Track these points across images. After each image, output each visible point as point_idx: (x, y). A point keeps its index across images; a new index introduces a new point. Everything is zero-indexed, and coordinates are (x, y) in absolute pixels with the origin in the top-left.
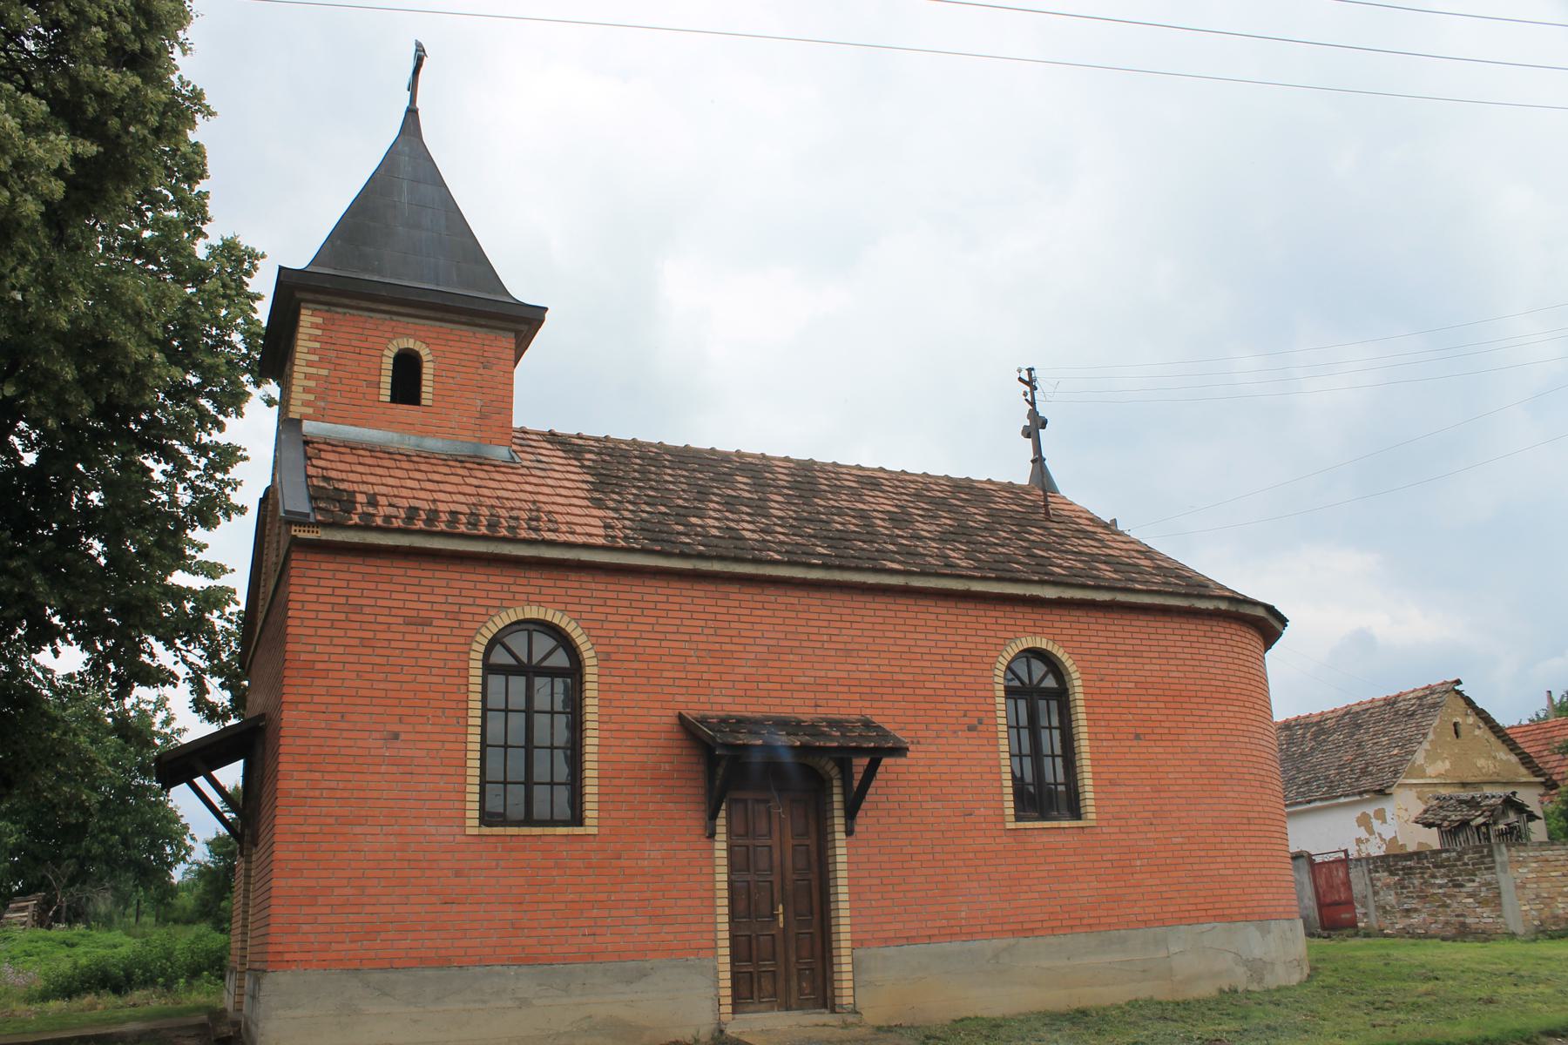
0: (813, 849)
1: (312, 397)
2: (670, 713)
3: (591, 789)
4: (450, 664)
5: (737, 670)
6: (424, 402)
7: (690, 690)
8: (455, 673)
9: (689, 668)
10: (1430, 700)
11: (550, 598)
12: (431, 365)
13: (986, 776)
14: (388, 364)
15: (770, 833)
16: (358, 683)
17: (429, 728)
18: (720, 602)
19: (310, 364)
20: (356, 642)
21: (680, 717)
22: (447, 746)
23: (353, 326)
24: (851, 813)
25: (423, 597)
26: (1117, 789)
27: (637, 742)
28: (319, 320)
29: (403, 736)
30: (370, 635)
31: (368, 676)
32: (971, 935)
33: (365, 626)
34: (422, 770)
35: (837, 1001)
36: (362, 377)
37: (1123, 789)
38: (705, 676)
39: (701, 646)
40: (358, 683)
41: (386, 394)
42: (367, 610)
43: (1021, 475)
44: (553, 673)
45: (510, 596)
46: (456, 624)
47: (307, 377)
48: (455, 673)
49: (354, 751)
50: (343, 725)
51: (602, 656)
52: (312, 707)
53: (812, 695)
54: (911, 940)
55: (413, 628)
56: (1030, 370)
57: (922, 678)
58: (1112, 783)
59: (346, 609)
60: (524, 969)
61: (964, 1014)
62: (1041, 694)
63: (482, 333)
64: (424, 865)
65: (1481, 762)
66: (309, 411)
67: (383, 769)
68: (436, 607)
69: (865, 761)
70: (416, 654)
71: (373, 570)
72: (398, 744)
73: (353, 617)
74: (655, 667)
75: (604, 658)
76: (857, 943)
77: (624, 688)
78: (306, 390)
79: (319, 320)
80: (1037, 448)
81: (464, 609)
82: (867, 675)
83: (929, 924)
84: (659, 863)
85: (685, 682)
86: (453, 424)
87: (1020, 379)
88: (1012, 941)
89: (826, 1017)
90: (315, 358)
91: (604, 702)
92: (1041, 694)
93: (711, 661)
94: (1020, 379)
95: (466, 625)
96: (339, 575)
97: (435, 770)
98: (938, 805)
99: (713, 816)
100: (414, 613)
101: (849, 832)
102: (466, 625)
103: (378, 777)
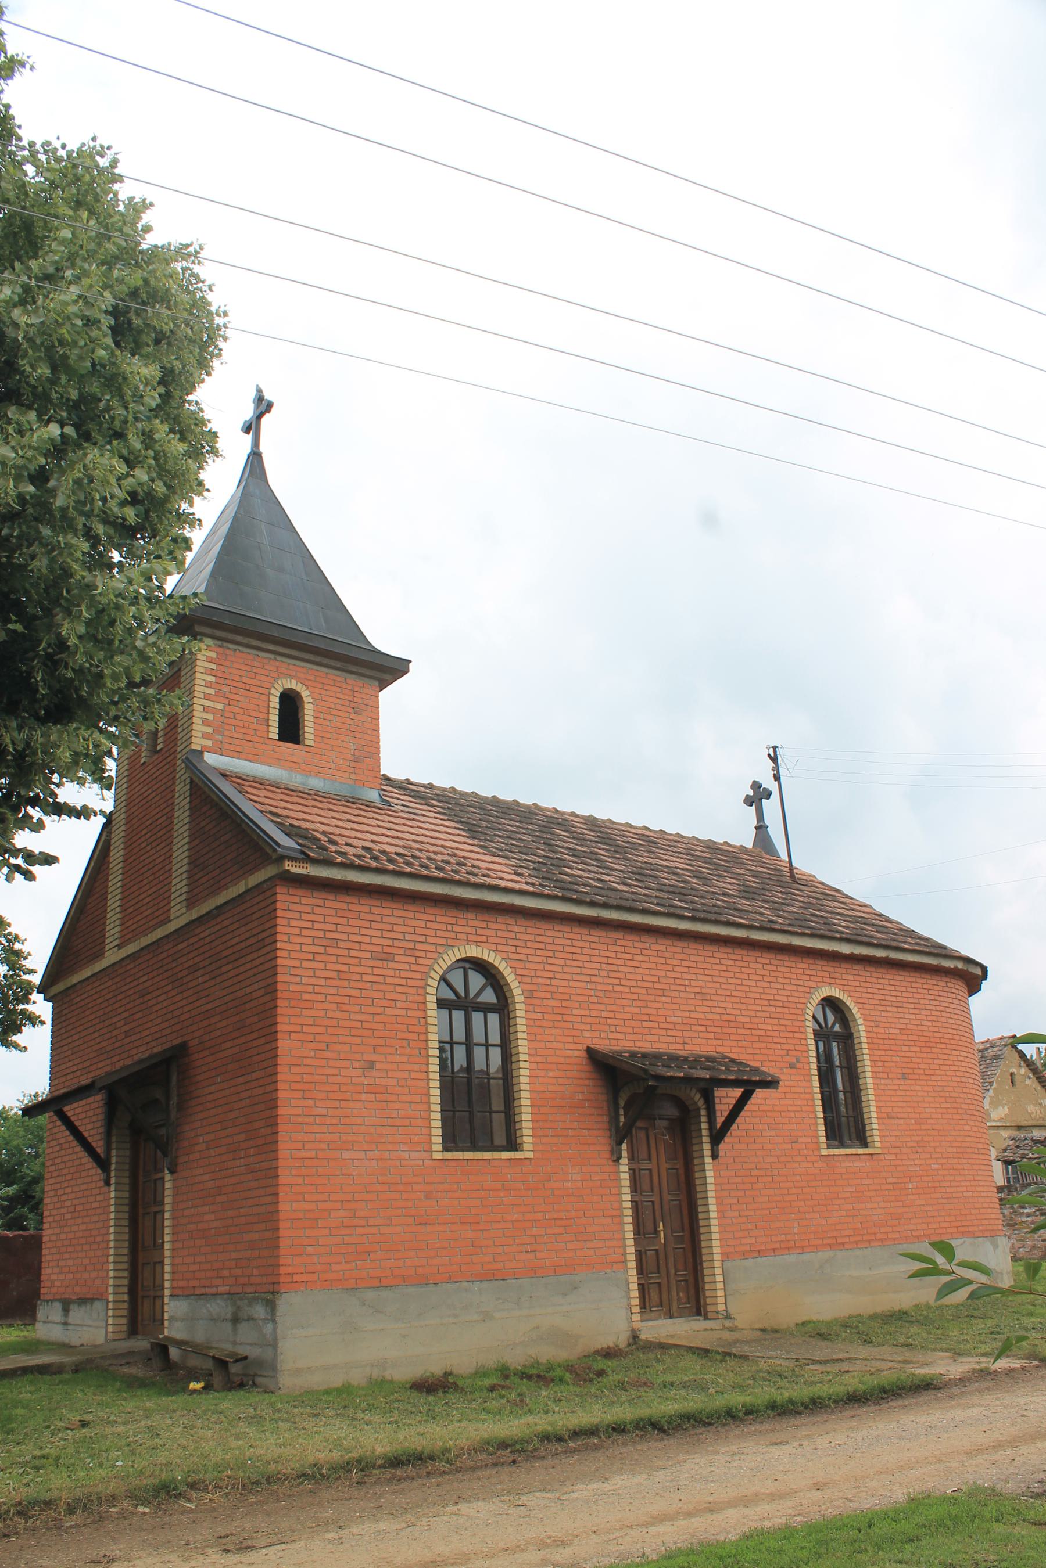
0: (681, 1172)
1: (210, 730)
2: (580, 1047)
3: (526, 1116)
4: (411, 998)
5: (627, 1009)
6: (307, 742)
7: (594, 1027)
8: (415, 1006)
9: (591, 1006)
10: (991, 1052)
11: (484, 939)
12: (311, 706)
13: (805, 1108)
14: (275, 702)
15: (649, 1159)
16: (339, 1014)
17: (398, 1058)
18: (610, 948)
19: (207, 697)
20: (334, 975)
21: (589, 1051)
22: (414, 1075)
23: (244, 662)
24: (717, 1137)
25: (386, 934)
26: (892, 1121)
27: (557, 1073)
28: (213, 655)
29: (378, 1066)
30: (345, 968)
31: (346, 1008)
32: (802, 1250)
33: (340, 960)
34: (394, 1098)
35: (710, 1308)
36: (253, 713)
37: (897, 1121)
38: (604, 1014)
39: (599, 987)
40: (339, 1014)
41: (274, 732)
42: (341, 944)
43: (745, 838)
44: (486, 1009)
45: (453, 935)
46: (412, 960)
47: (205, 709)
48: (415, 1006)
49: (339, 1079)
50: (329, 1054)
51: (527, 994)
52: (302, 1037)
53: (680, 1034)
54: (760, 1253)
55: (379, 963)
56: (775, 748)
57: (756, 1020)
58: (889, 1116)
59: (324, 942)
60: (485, 1285)
61: (805, 1319)
62: (837, 1034)
63: (352, 679)
64: (401, 1188)
65: (1031, 1108)
66: (209, 743)
67: (364, 1096)
68: (396, 943)
69: (738, 1092)
70: (382, 987)
71: (344, 906)
72: (374, 1073)
73: (330, 950)
74: (578, 1002)
75: (529, 995)
76: (726, 1256)
77: (544, 1024)
78: (205, 722)
79: (213, 655)
80: (760, 816)
81: (419, 946)
82: (718, 1017)
83: (774, 1239)
84: (579, 1184)
85: (589, 1020)
86: (332, 766)
87: (769, 755)
88: (831, 1253)
89: (698, 1324)
90: (212, 691)
91: (532, 1037)
92: (837, 1034)
93: (606, 1001)
94: (769, 755)
95: (421, 961)
96: (317, 910)
97: (404, 1098)
98: (773, 1133)
99: (620, 1143)
100: (379, 949)
101: (715, 1156)
102: (421, 961)
103: (359, 1105)
